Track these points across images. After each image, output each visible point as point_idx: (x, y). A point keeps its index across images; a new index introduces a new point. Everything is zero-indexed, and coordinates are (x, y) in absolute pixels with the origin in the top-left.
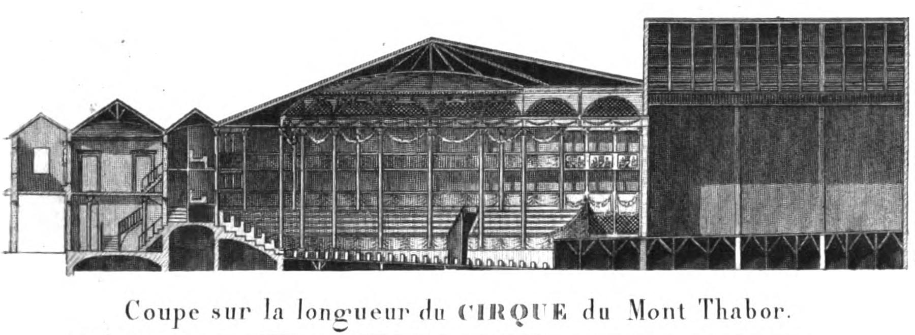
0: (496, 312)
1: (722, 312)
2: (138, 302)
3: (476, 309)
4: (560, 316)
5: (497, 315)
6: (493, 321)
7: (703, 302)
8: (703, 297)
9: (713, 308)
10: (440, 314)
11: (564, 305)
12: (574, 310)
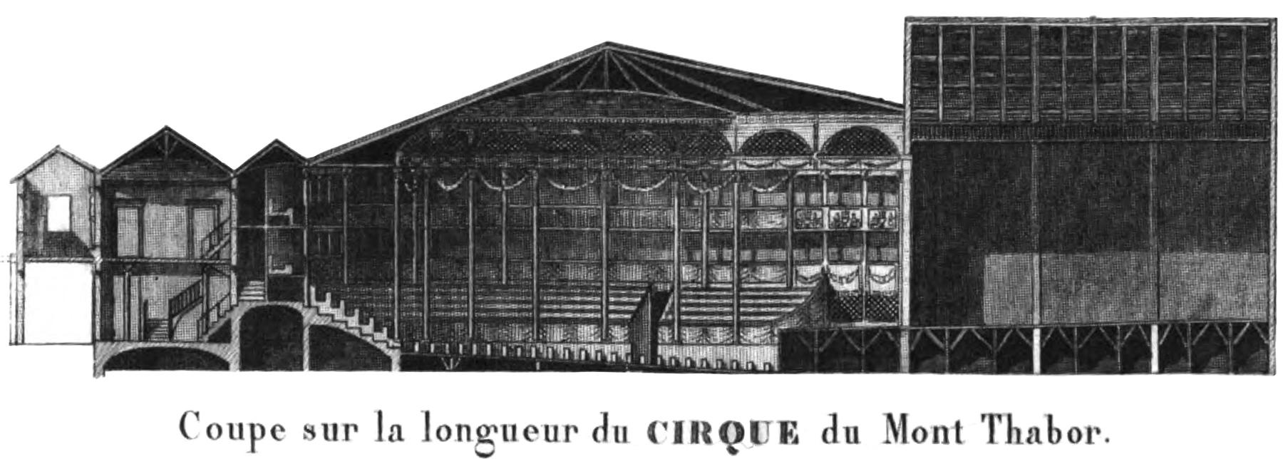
0: (700, 432)
2: (197, 414)
3: (672, 427)
4: (790, 440)
5: (700, 437)
6: (695, 445)
8: (987, 411)
9: (1001, 429)
10: (622, 435)
11: (794, 424)
12: (809, 431)
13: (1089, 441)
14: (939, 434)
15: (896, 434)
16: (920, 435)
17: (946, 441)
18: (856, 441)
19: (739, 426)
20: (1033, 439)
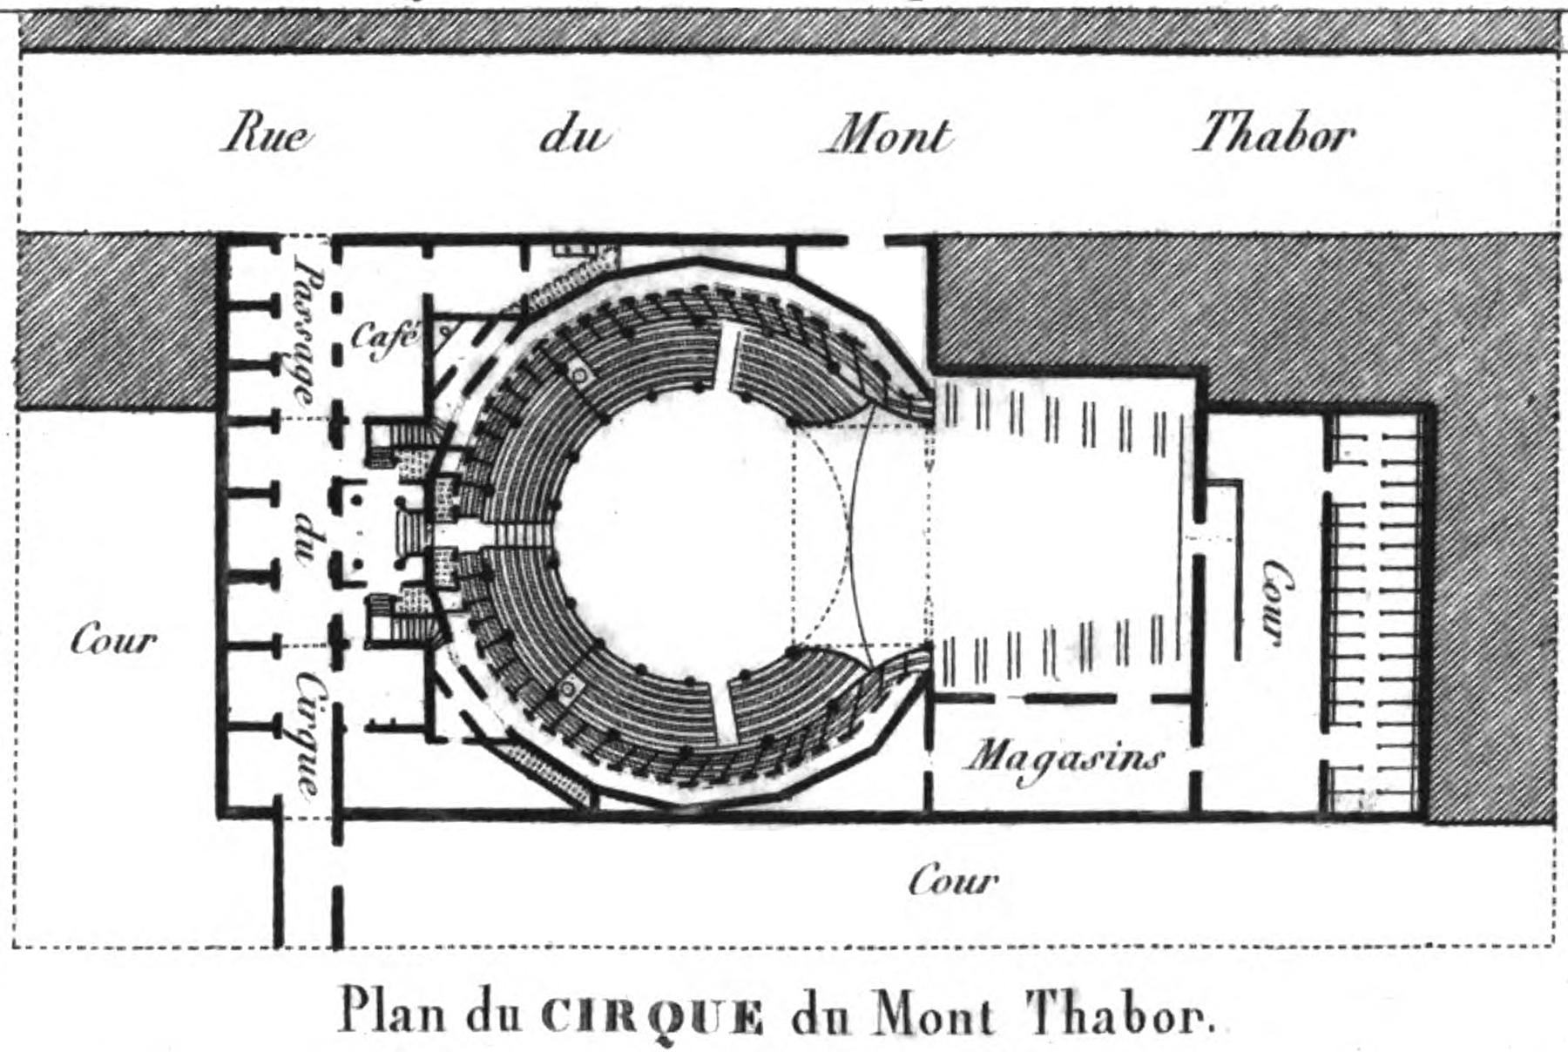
0: (619, 1015)
1: (1076, 1017)
3: (576, 1008)
4: (749, 1027)
5: (620, 1022)
6: (611, 1033)
7: (1035, 997)
8: (1036, 986)
9: (1055, 1010)
10: (510, 1020)
11: (758, 1005)
12: (775, 1017)
13: (1186, 1029)
14: (960, 1021)
15: (893, 1022)
16: (931, 1022)
17: (968, 1030)
18: (515, 1027)
19: (676, 1009)
20: (400, 1026)
